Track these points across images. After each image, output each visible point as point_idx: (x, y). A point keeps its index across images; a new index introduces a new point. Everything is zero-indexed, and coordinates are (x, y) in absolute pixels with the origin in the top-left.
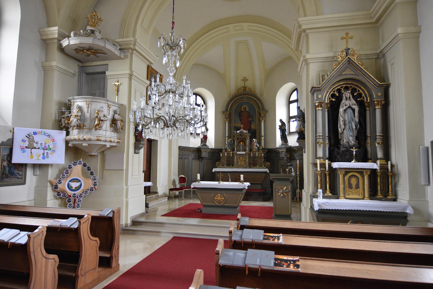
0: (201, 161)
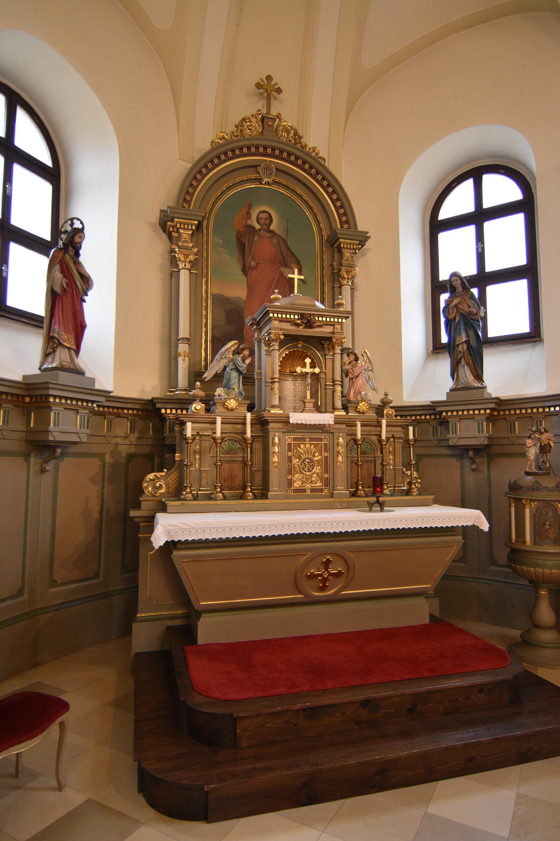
0: (38, 468)
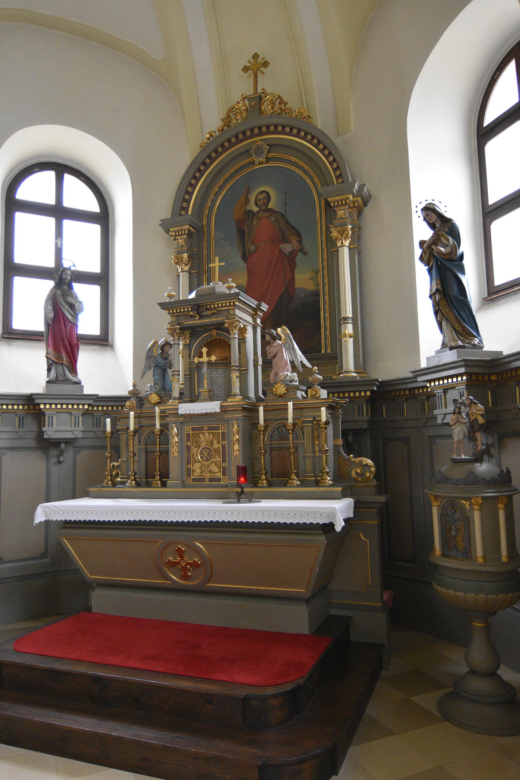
0: (55, 459)
